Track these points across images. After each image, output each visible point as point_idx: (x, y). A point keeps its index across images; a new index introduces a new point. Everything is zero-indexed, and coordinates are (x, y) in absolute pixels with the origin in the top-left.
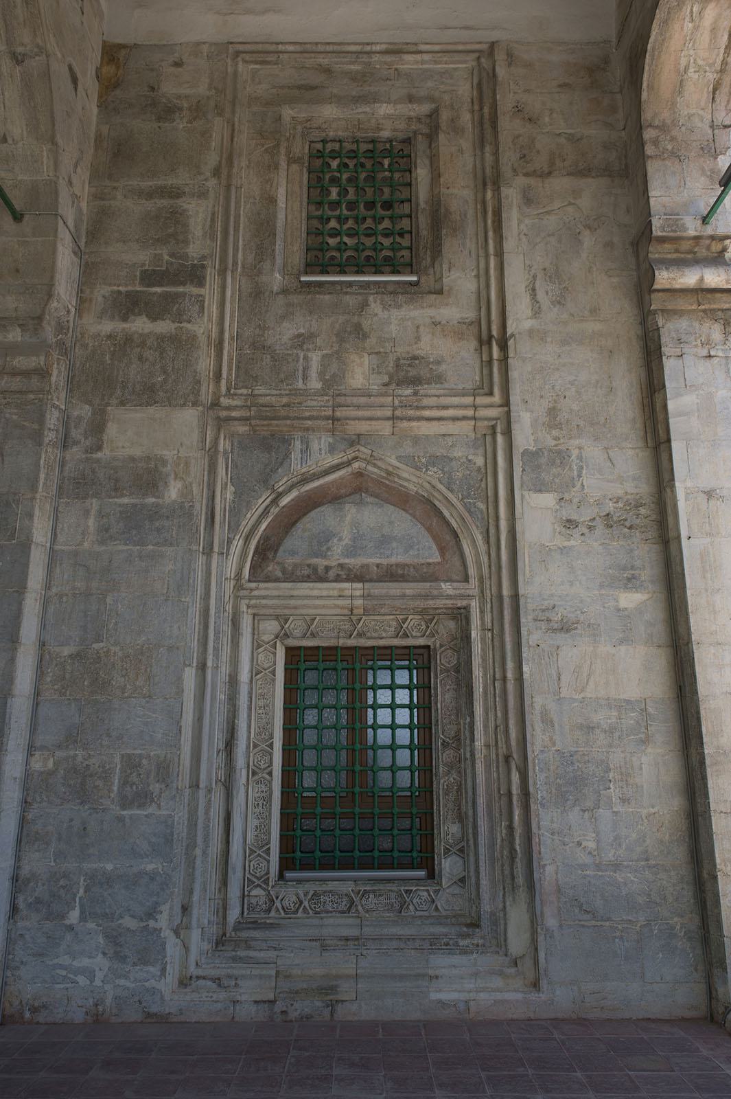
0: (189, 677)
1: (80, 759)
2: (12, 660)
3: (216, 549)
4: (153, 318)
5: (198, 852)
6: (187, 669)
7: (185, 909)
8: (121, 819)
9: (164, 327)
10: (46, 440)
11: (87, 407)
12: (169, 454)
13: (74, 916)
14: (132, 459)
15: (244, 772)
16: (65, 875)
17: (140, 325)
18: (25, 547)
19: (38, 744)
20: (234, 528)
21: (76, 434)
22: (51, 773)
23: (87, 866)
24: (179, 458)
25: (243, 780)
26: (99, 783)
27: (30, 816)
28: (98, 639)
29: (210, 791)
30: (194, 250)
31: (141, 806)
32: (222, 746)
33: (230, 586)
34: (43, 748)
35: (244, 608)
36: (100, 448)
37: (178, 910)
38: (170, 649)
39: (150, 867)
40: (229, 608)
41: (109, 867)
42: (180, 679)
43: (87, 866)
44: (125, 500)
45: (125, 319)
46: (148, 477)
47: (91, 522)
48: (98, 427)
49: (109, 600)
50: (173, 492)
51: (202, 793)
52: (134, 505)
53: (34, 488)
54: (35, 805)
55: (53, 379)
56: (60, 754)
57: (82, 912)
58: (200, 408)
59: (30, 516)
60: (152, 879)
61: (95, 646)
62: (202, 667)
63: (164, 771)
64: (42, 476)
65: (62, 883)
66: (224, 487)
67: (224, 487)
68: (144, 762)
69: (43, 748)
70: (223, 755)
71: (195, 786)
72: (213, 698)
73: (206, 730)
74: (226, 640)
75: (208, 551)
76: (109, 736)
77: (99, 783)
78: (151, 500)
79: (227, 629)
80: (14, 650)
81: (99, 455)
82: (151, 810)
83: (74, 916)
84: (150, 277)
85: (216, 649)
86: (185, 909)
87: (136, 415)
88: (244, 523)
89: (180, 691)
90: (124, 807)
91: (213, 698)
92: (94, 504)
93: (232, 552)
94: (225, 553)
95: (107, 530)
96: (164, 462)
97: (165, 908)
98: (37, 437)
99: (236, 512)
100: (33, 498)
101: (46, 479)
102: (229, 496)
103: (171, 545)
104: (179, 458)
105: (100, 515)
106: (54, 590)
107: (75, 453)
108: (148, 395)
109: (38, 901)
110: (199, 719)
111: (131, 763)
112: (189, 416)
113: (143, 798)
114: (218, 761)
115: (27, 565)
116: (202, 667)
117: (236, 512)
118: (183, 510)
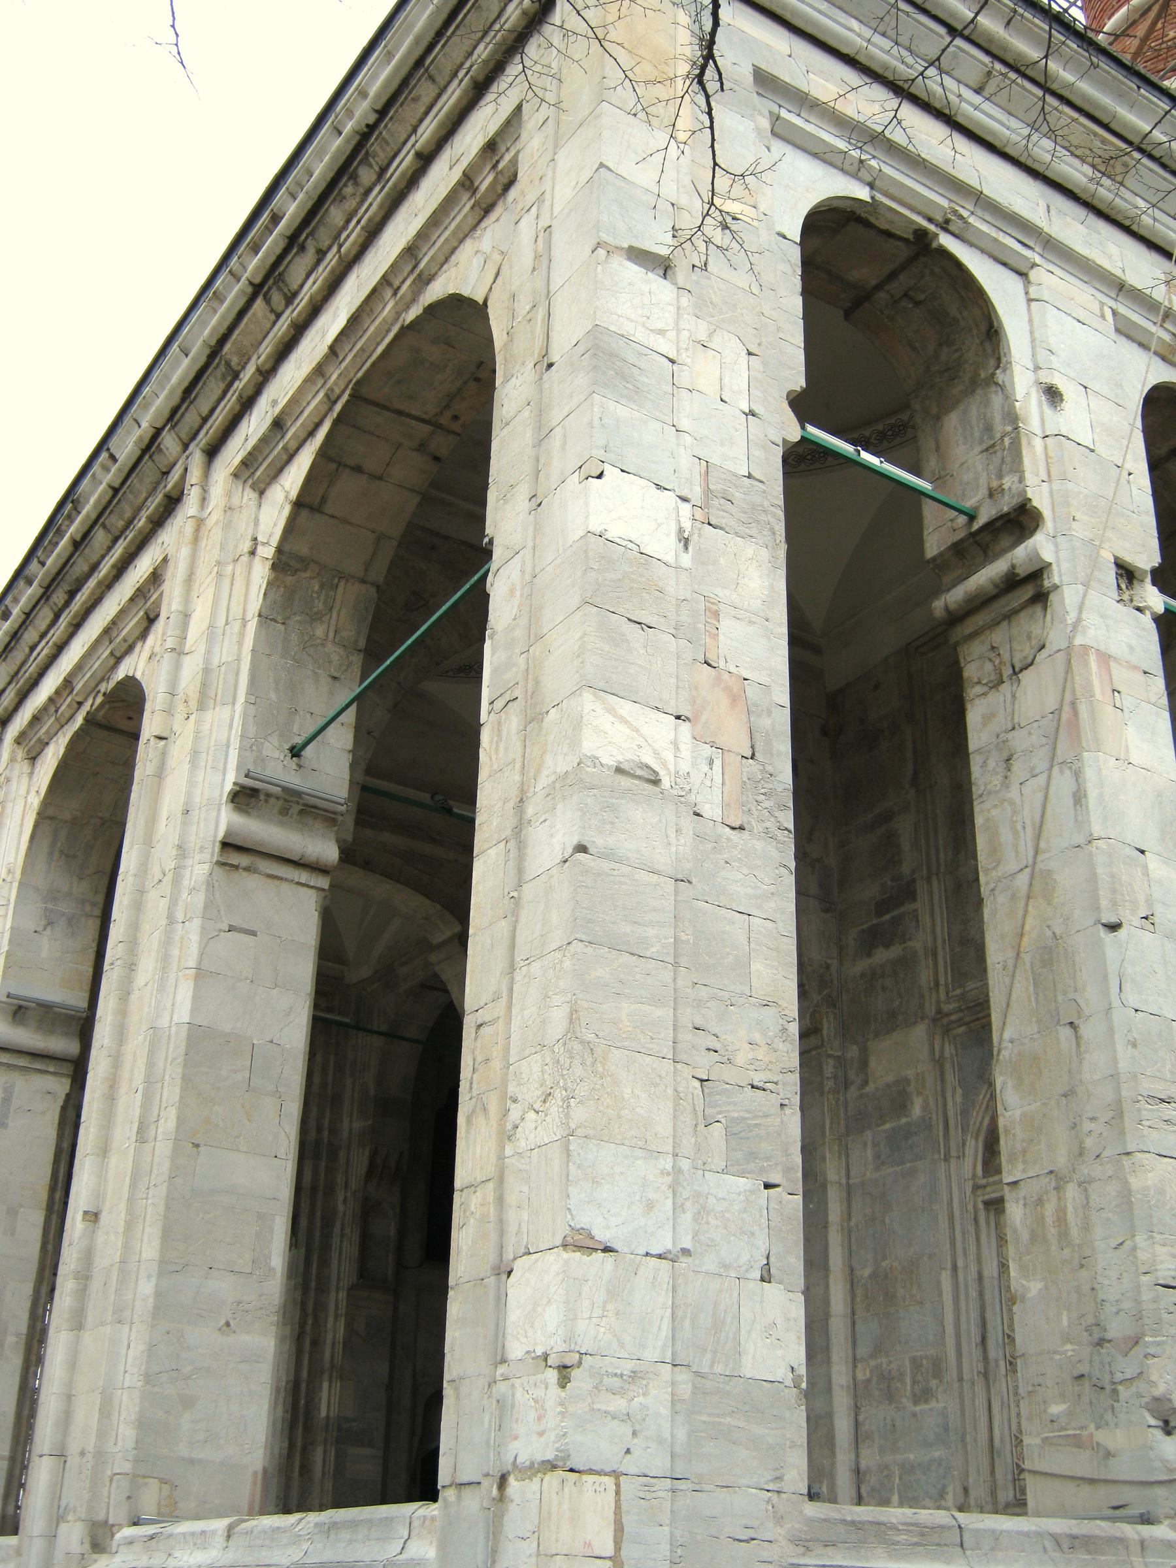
0: (946, 1279)
1: (884, 1366)
2: (827, 1287)
3: (953, 1153)
4: (887, 946)
5: (968, 1438)
6: (943, 1273)
7: (966, 1490)
8: (914, 1415)
9: (895, 951)
10: (827, 1089)
11: (855, 1047)
12: (910, 1073)
14: (888, 1086)
15: (1002, 1364)
16: (886, 1467)
17: (882, 956)
19: (858, 1357)
20: (965, 1130)
21: (852, 1075)
22: (869, 1381)
23: (899, 1457)
24: (918, 1074)
25: (1003, 1371)
26: (898, 1385)
27: (861, 1418)
28: (884, 1258)
29: (973, 1383)
30: (906, 868)
31: (926, 1401)
32: (979, 1340)
33: (969, 1186)
34: (862, 1359)
35: (981, 1206)
36: (866, 1083)
37: (959, 1490)
38: (931, 1256)
39: (937, 1454)
40: (970, 1208)
41: (912, 1457)
42: (939, 1282)
43: (899, 1457)
44: (887, 1126)
45: (869, 955)
47: (869, 1153)
49: (887, 1221)
50: (917, 1110)
51: (966, 1386)
52: (894, 1129)
53: (823, 1134)
54: (863, 1409)
55: (825, 1032)
56: (873, 1363)
57: (900, 1497)
58: (926, 1021)
59: (824, 1158)
60: (939, 1464)
61: (884, 1264)
62: (955, 1268)
63: (938, 1368)
64: (828, 1122)
65: (885, 1473)
66: (954, 1090)
67: (954, 1090)
68: (924, 1362)
69: (862, 1359)
70: (980, 1348)
71: (961, 1379)
72: (967, 1296)
73: (963, 1326)
74: (972, 1239)
75: (947, 1159)
76: (900, 1342)
77: (898, 1385)
78: (904, 1120)
79: (971, 1229)
80: (827, 1277)
81: (867, 1089)
82: (933, 1404)
84: (882, 907)
85: (964, 1250)
86: (966, 1490)
88: (972, 1123)
89: (940, 1294)
90: (916, 1403)
91: (967, 1296)
93: (967, 1152)
94: (961, 1156)
95: (879, 1157)
96: (907, 1081)
97: (950, 1489)
99: (965, 1113)
100: (824, 1143)
101: (831, 1124)
102: (959, 1099)
103: (921, 1159)
104: (918, 1074)
105: (875, 1144)
106: (854, 1220)
107: (853, 1092)
109: (873, 1489)
110: (957, 1319)
111: (916, 1363)
112: (920, 1031)
114: (977, 1353)
115: (826, 1203)
116: (955, 1268)
117: (965, 1113)
118: (926, 1124)
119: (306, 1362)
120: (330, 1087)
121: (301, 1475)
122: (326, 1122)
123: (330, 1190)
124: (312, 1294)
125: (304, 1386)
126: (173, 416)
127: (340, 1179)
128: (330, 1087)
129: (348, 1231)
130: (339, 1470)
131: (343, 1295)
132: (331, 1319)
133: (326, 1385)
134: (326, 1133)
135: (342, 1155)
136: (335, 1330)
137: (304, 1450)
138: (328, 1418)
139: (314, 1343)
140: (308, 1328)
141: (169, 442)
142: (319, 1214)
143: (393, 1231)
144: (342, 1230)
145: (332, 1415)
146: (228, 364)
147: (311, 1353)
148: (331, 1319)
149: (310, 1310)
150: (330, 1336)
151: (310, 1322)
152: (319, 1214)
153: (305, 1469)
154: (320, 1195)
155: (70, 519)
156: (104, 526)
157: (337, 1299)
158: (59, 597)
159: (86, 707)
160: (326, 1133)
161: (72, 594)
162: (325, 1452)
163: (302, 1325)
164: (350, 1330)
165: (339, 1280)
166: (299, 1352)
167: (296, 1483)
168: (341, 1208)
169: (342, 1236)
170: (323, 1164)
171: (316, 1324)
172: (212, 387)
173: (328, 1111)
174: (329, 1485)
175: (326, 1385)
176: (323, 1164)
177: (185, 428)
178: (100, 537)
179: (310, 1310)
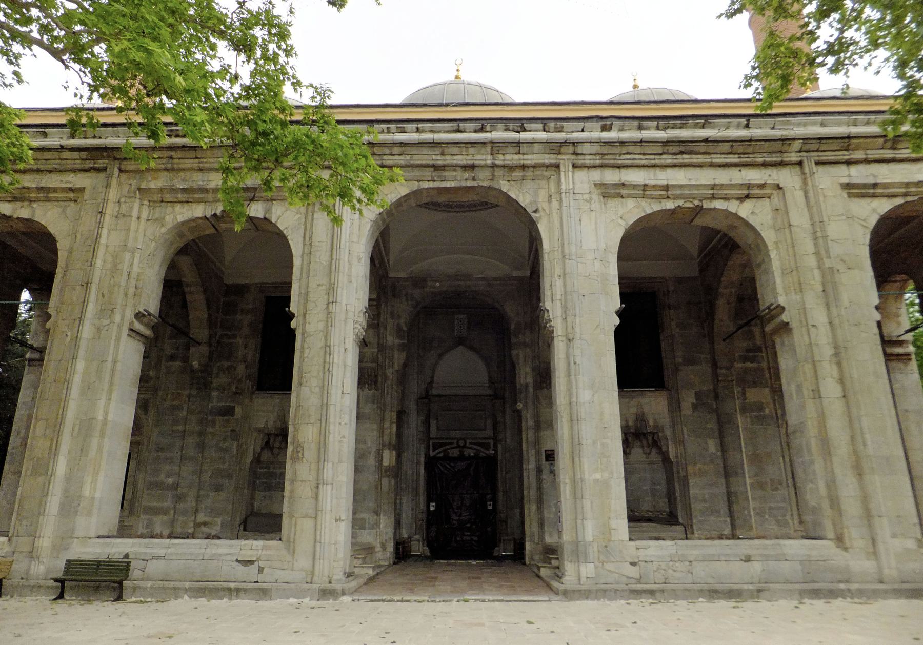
4: (752, 362)
9: (754, 365)
12: (764, 401)
13: (767, 516)
17: (749, 365)
18: (738, 426)
46: (760, 407)
48: (744, 394)
50: (767, 411)
63: (780, 483)
83: (767, 516)
84: (749, 351)
87: (754, 390)
92: (748, 414)
98: (734, 398)
108: (755, 384)
113: (777, 489)
126: (806, 140)
141: (797, 145)
146: (849, 145)
155: (696, 126)
156: (732, 146)
158: (673, 149)
159: (680, 203)
161: (682, 153)
172: (835, 145)
177: (807, 147)
178: (726, 147)
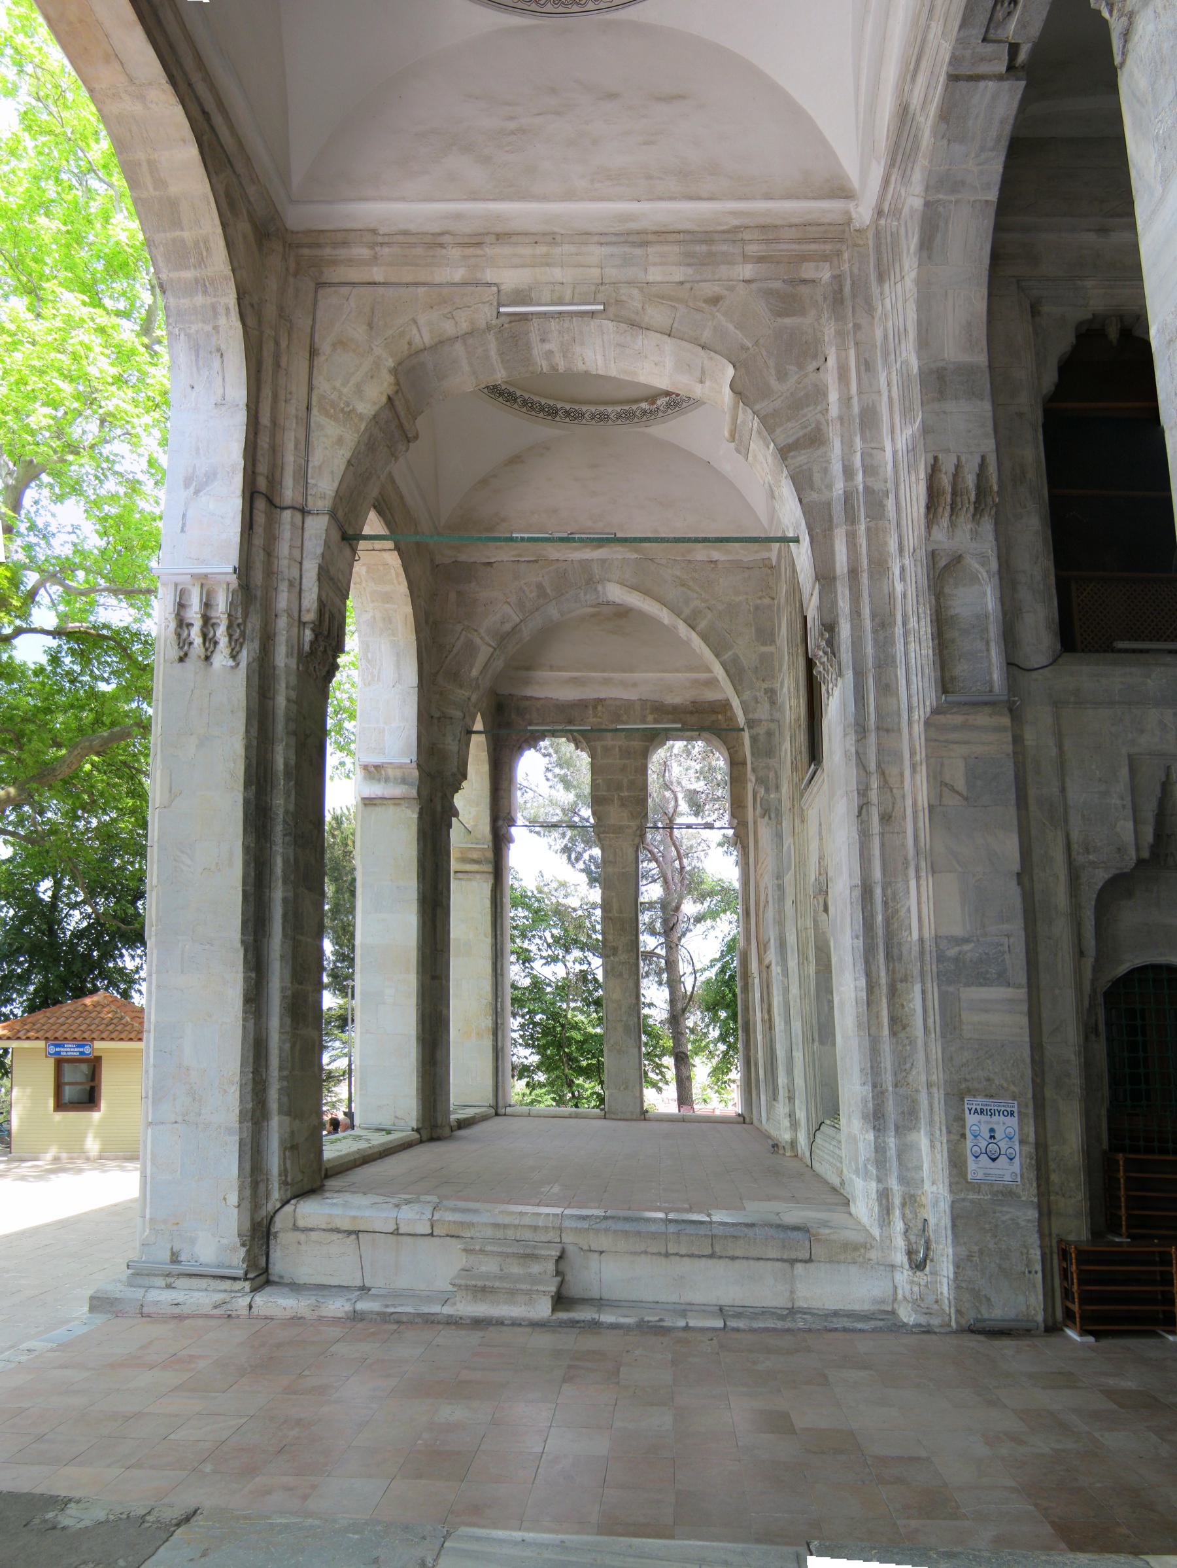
119: (876, 852)
120: (855, 401)
121: (893, 1033)
122: (857, 460)
123: (879, 566)
124: (872, 738)
125: (878, 891)
127: (893, 545)
128: (855, 401)
129: (912, 624)
130: (950, 1024)
131: (918, 729)
132: (907, 773)
133: (913, 883)
134: (859, 477)
135: (890, 503)
136: (916, 789)
137: (893, 991)
138: (921, 940)
139: (886, 818)
140: (874, 795)
142: (866, 612)
143: (991, 602)
144: (904, 624)
145: (926, 935)
147: (882, 834)
148: (907, 773)
149: (872, 766)
150: (909, 802)
151: (874, 785)
152: (866, 612)
153: (898, 1023)
154: (865, 579)
157: (912, 734)
160: (859, 477)
162: (923, 992)
163: (863, 792)
164: (939, 783)
165: (910, 709)
166: (864, 835)
167: (886, 1047)
168: (899, 587)
169: (906, 635)
170: (862, 528)
171: (885, 785)
173: (858, 440)
174: (936, 1050)
175: (913, 883)
176: (862, 528)
179: (872, 766)
